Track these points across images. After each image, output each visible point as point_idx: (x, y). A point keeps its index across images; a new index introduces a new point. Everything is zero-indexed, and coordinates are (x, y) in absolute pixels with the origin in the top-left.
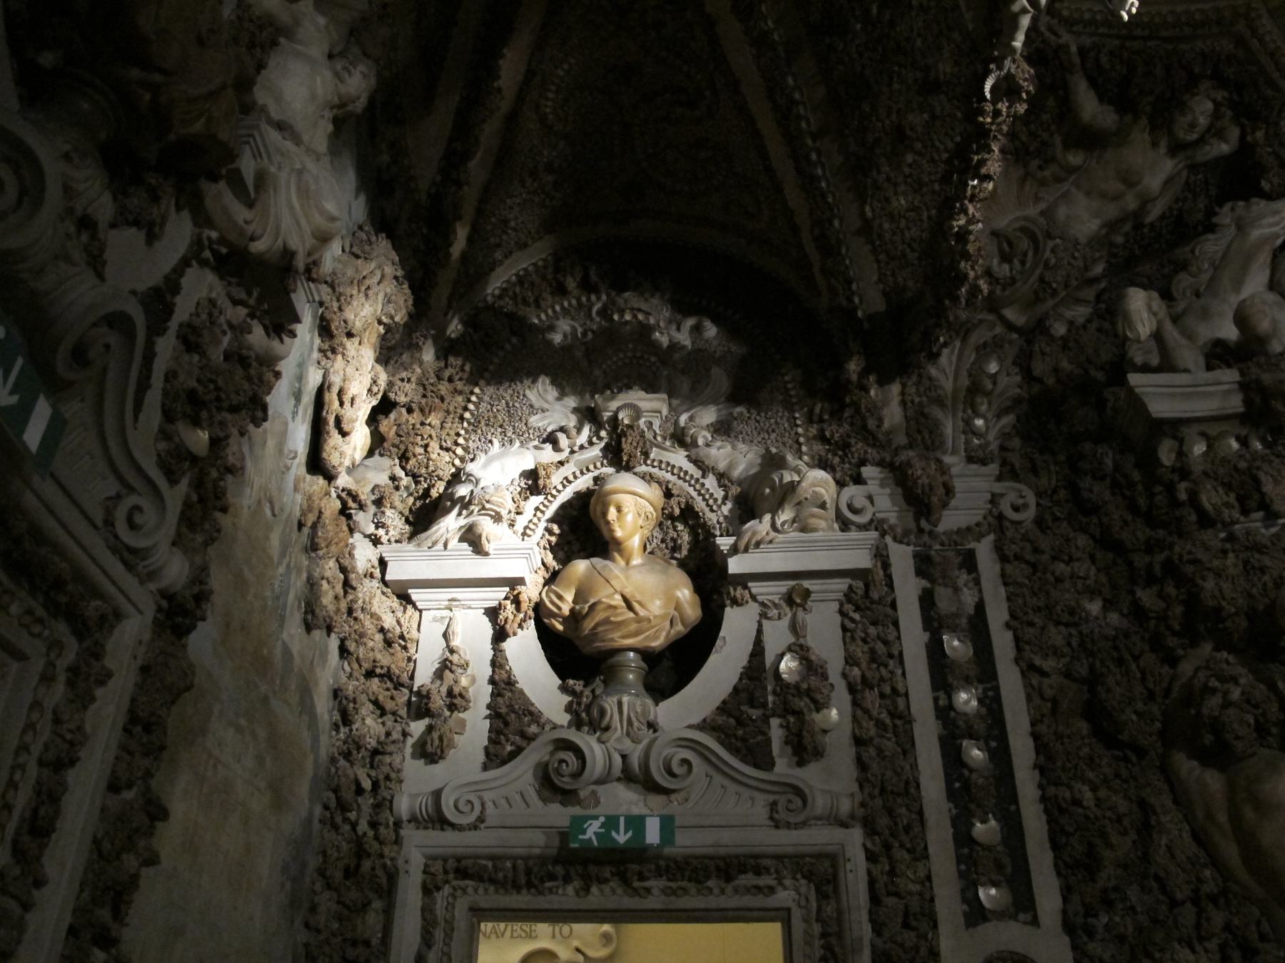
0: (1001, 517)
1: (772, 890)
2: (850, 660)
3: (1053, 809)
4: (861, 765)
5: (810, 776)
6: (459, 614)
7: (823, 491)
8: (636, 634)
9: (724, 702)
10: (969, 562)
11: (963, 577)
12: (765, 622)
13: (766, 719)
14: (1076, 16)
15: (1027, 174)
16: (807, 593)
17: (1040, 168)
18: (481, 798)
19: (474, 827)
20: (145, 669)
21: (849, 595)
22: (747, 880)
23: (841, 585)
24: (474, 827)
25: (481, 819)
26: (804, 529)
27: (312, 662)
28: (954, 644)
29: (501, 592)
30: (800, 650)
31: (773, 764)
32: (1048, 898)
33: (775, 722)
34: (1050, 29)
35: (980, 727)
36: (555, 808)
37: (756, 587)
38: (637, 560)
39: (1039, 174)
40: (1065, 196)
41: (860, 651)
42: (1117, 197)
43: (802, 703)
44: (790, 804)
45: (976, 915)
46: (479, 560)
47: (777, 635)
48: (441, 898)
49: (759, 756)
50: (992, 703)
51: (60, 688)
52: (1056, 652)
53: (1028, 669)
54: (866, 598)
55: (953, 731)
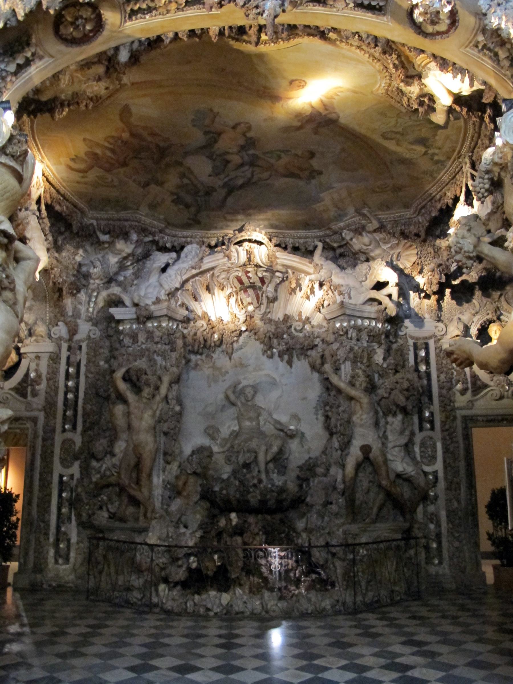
2: (48, 373)
3: (84, 409)
4: (46, 398)
5: (35, 400)
10: (80, 348)
11: (78, 352)
13: (27, 387)
21: (50, 358)
22: (21, 422)
23: (48, 355)
28: (71, 370)
30: (36, 371)
32: (79, 428)
35: (74, 390)
43: (34, 384)
44: (29, 407)
45: (64, 430)
47: (33, 366)
49: (24, 395)
52: (92, 373)
53: (87, 377)
54: (54, 358)
55: (67, 390)
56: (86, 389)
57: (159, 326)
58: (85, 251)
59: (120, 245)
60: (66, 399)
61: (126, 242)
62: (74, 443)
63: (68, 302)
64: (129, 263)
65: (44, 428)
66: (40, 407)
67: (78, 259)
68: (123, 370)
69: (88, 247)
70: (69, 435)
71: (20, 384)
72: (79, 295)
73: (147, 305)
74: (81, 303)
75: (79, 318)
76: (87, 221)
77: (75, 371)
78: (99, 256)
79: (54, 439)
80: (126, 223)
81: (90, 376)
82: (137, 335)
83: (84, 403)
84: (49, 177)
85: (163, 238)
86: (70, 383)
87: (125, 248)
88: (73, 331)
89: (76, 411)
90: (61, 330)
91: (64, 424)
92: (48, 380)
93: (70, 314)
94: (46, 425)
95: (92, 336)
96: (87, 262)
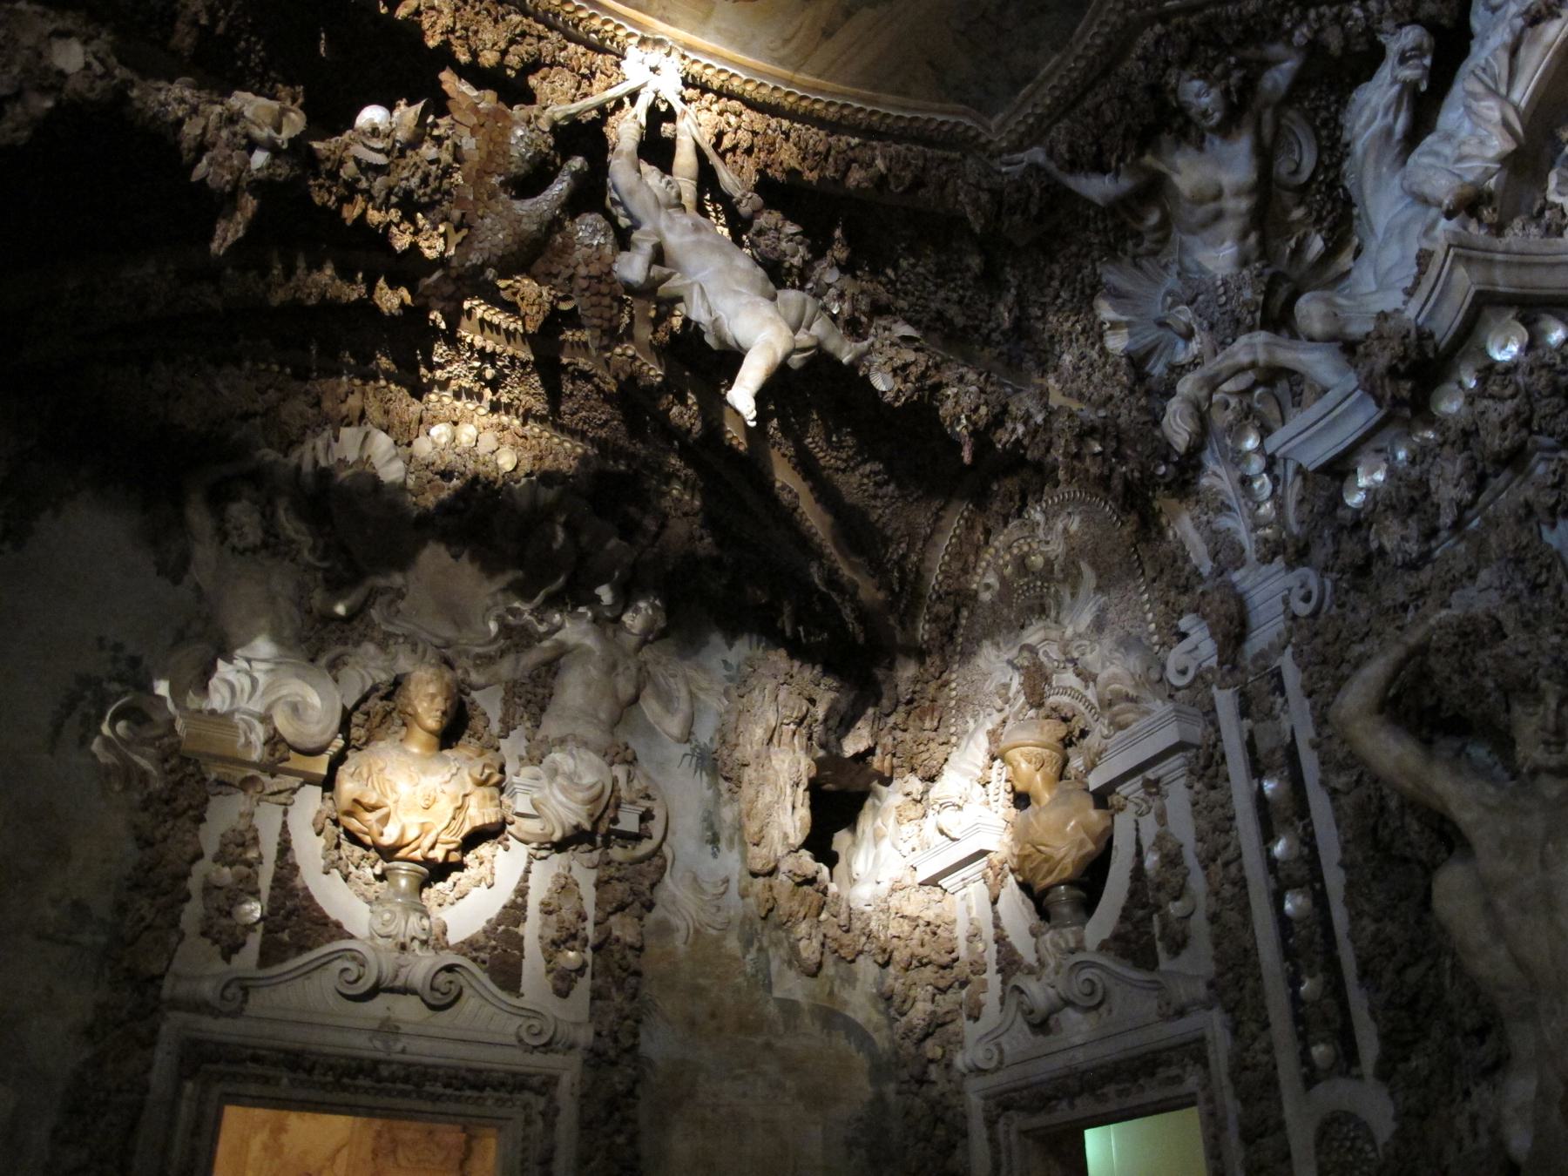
0: (1295, 617)
1: (1178, 1080)
5: (1183, 963)
6: (971, 888)
7: (1117, 686)
8: (1050, 872)
9: (1124, 909)
11: (1280, 700)
12: (1141, 820)
14: (1014, 137)
15: (1134, 257)
16: (1156, 782)
17: (1137, 245)
18: (998, 1045)
19: (997, 1069)
20: (584, 1096)
22: (1162, 1073)
24: (997, 1069)
25: (1001, 1062)
26: (1122, 727)
27: (831, 993)
28: (1269, 786)
29: (981, 864)
31: (1156, 963)
32: (1369, 1047)
33: (1155, 917)
34: (1009, 164)
35: (1302, 872)
36: (1041, 1038)
37: (1124, 790)
38: (1046, 797)
39: (1141, 250)
40: (1182, 244)
41: (1205, 825)
42: (1219, 216)
46: (956, 845)
48: (1001, 1127)
50: (1309, 840)
51: (540, 1125)
53: (1334, 793)
55: (1281, 879)
56: (1344, 850)
57: (1489, 370)
58: (1117, 295)
59: (1188, 173)
60: (1283, 921)
61: (1200, 149)
62: (1362, 1125)
63: (1185, 527)
64: (1317, 245)
65: (1234, 1080)
66: (1201, 991)
67: (1117, 343)
68: (1375, 671)
69: (1112, 276)
70: (1337, 1094)
71: (1126, 915)
72: (1205, 482)
73: (1383, 316)
74: (1224, 508)
75: (1239, 561)
76: (1011, 168)
77: (1286, 786)
78: (1171, 281)
79: (1281, 1125)
80: (1131, 65)
81: (1340, 781)
82: (1423, 483)
83: (1352, 919)
84: (736, 85)
85: (1338, 20)
86: (1279, 848)
87: (1215, 171)
88: (1234, 631)
89: (1332, 965)
90: (1199, 645)
91: (1304, 1041)
92: (1207, 862)
93: (1206, 568)
94: (1239, 1067)
95: (1304, 610)
96: (1152, 335)
